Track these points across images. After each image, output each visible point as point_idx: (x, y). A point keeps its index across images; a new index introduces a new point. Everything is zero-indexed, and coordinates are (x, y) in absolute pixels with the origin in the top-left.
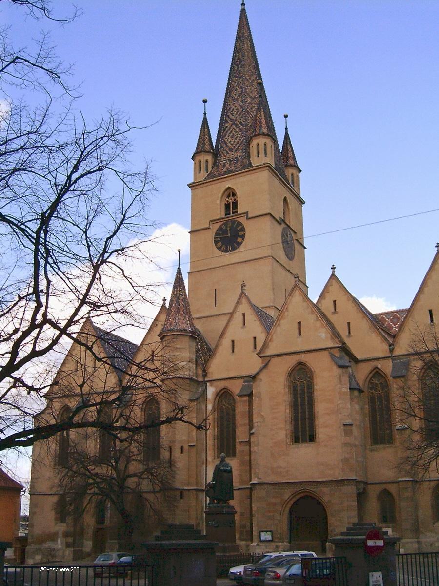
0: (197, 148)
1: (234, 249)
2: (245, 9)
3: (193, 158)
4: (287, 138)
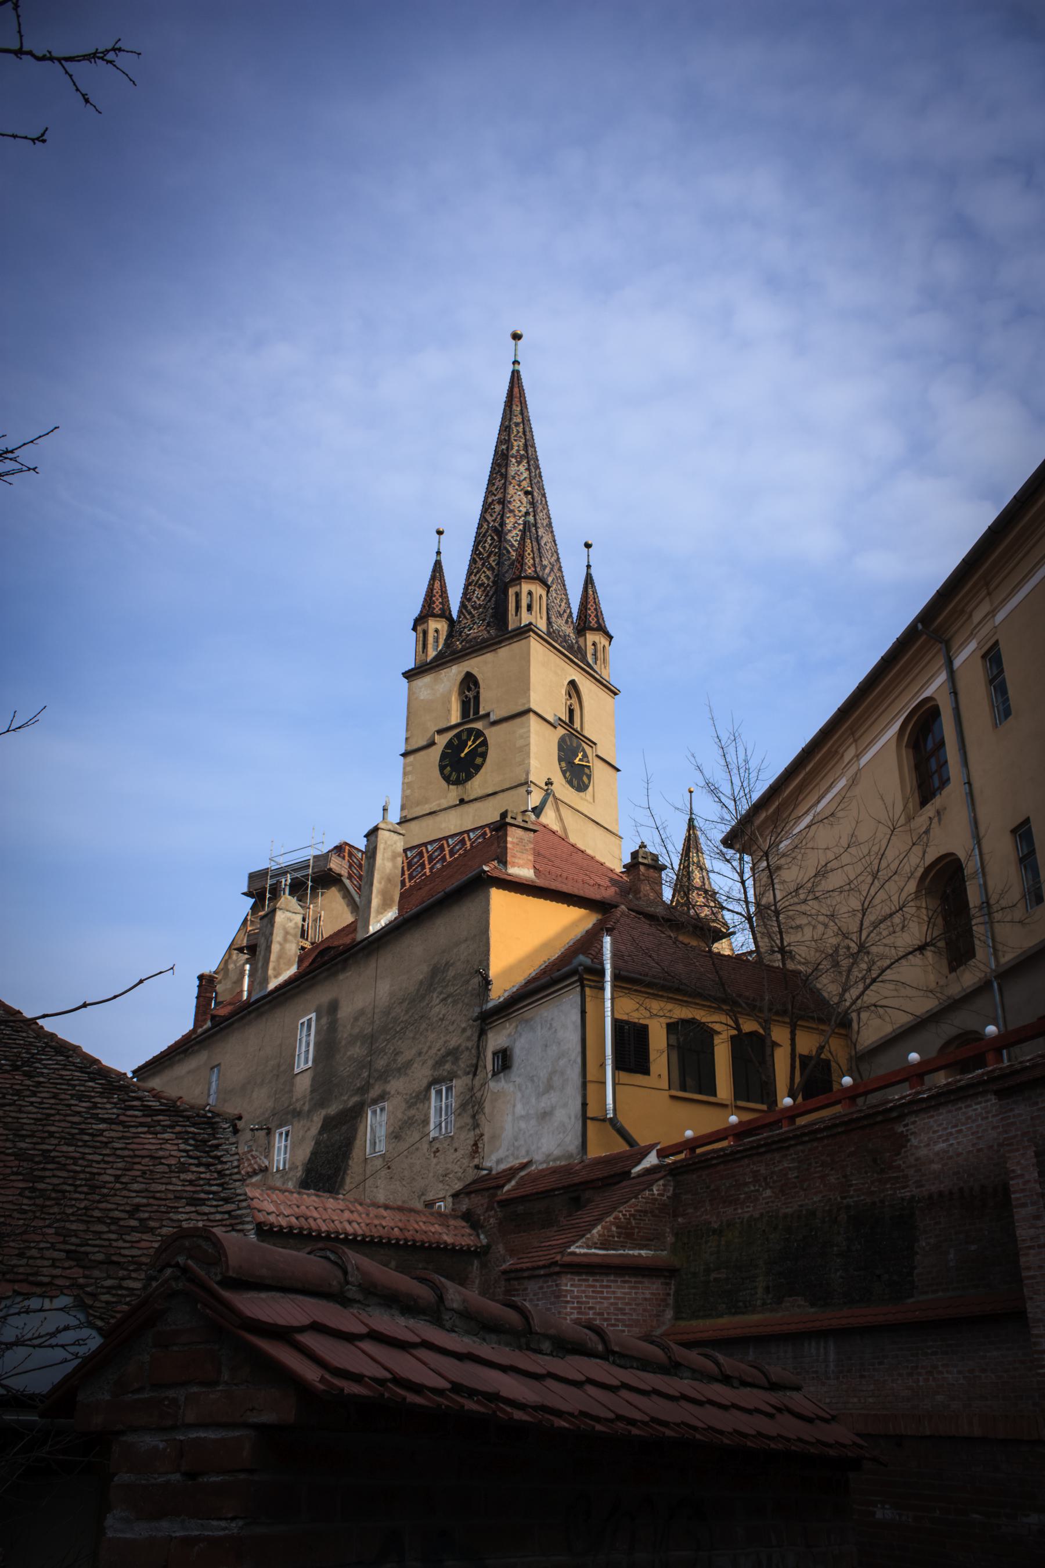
0: (421, 612)
1: (469, 777)
2: (518, 372)
3: (414, 629)
4: (589, 581)
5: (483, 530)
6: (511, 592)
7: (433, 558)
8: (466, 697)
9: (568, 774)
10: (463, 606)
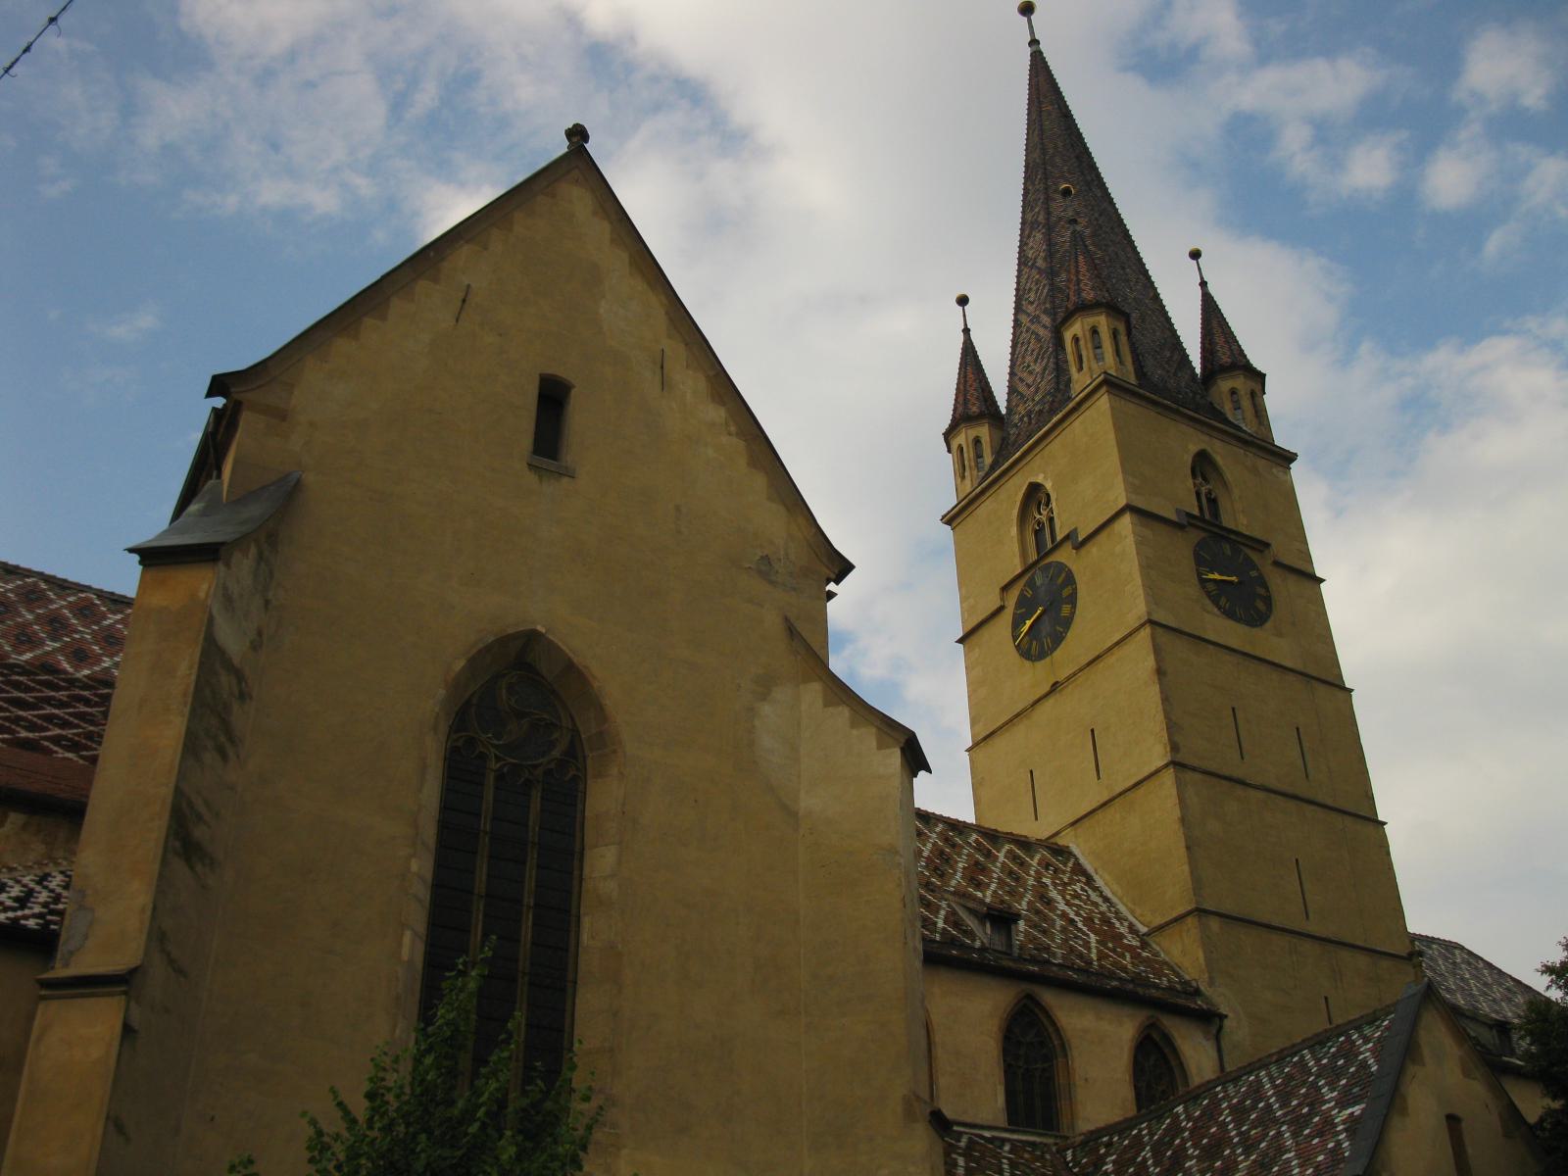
4: (1211, 311)
5: (1023, 281)
6: (1068, 336)
7: (961, 337)
8: (1039, 523)
9: (1223, 601)
10: (1012, 390)
